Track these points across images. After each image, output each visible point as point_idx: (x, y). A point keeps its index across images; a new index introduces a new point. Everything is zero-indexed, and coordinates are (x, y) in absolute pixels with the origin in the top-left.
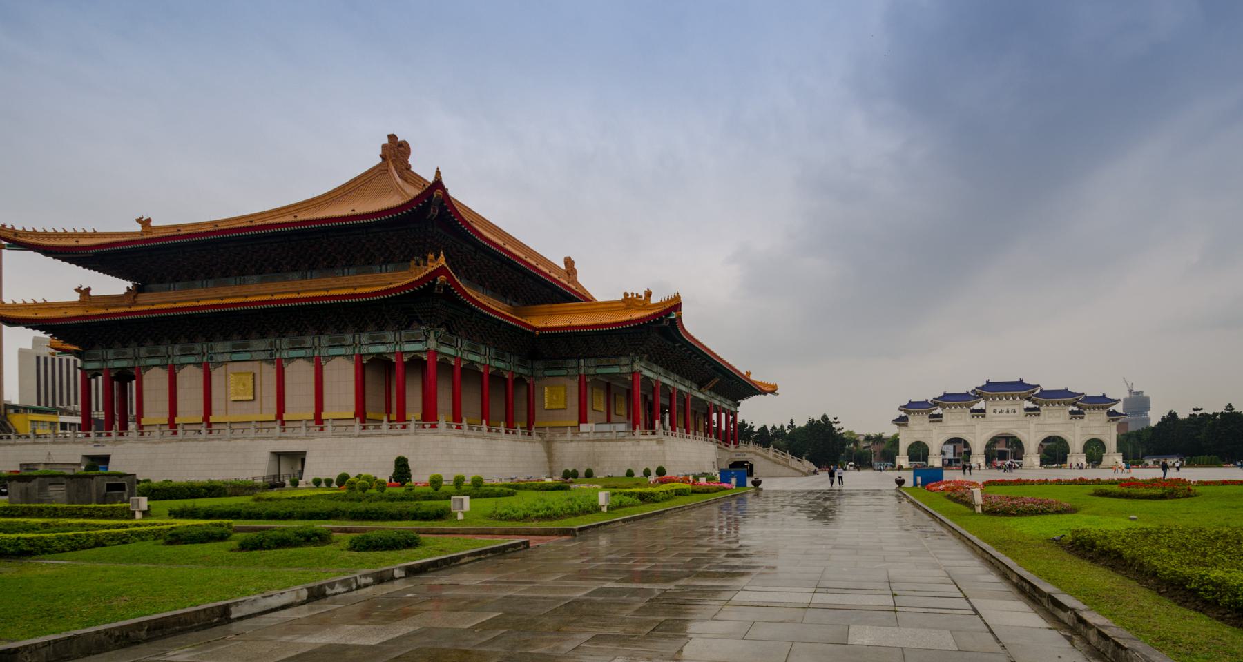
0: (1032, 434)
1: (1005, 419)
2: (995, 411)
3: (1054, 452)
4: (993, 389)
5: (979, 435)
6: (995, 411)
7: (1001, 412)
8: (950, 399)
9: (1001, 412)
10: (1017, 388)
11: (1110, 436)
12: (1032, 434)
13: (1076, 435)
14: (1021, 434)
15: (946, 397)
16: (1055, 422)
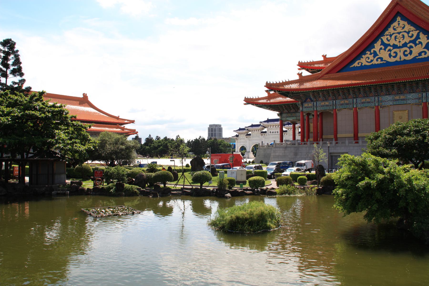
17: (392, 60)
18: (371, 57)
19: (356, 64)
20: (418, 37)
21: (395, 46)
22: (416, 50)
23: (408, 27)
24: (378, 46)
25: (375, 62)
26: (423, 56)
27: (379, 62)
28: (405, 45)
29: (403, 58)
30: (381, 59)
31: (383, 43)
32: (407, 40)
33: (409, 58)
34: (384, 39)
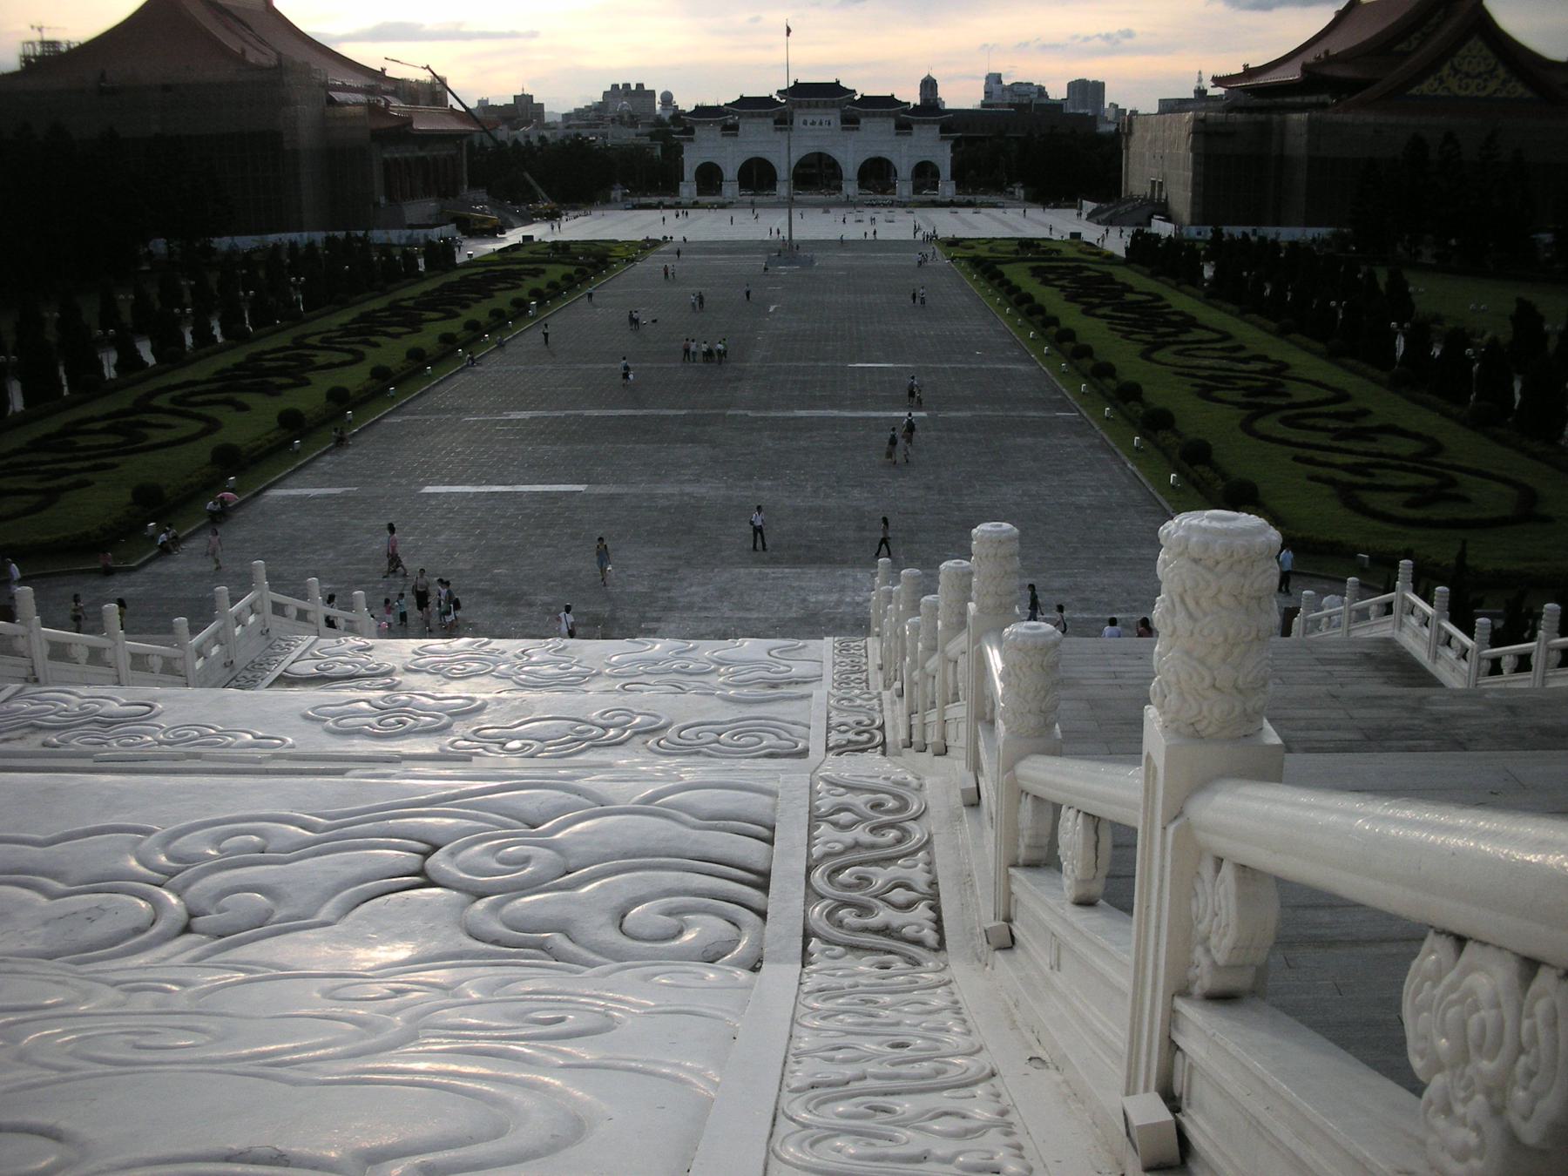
0: (850, 153)
1: (816, 134)
2: (805, 123)
3: (877, 175)
4: (800, 92)
5: (783, 154)
6: (805, 123)
7: (813, 123)
8: (747, 105)
9: (813, 123)
10: (827, 95)
11: (943, 157)
12: (850, 153)
13: (904, 154)
14: (837, 154)
15: (744, 102)
16: (876, 140)
17: (1463, 93)
18: (1436, 85)
19: (1414, 91)
20: (1495, 69)
21: (1467, 75)
22: (1492, 86)
23: (1486, 52)
24: (1446, 70)
25: (1439, 92)
26: (1499, 95)
27: (1445, 93)
28: (1479, 75)
29: (1476, 93)
30: (1448, 89)
31: (1453, 67)
32: (1482, 69)
33: (1483, 94)
34: (1456, 61)
